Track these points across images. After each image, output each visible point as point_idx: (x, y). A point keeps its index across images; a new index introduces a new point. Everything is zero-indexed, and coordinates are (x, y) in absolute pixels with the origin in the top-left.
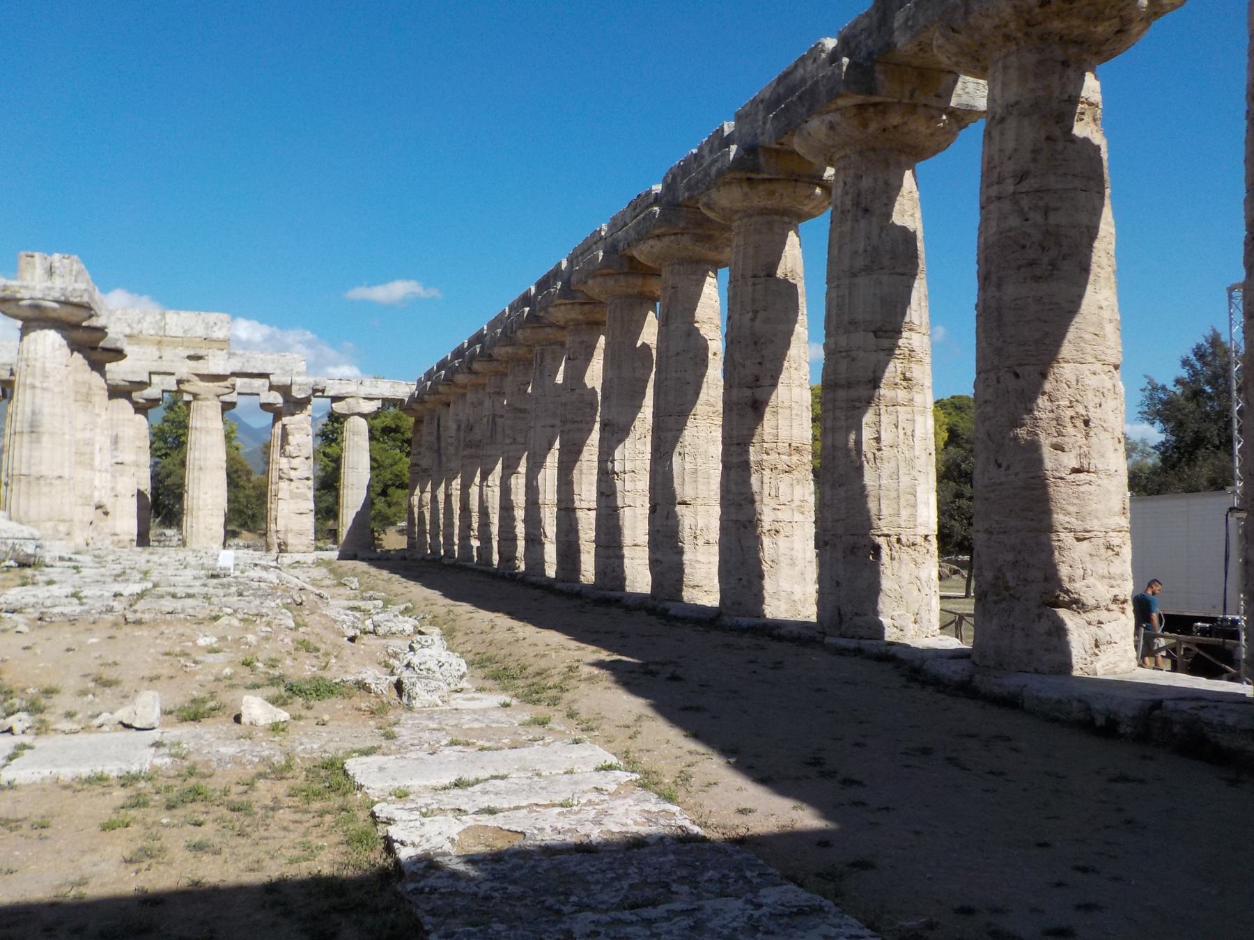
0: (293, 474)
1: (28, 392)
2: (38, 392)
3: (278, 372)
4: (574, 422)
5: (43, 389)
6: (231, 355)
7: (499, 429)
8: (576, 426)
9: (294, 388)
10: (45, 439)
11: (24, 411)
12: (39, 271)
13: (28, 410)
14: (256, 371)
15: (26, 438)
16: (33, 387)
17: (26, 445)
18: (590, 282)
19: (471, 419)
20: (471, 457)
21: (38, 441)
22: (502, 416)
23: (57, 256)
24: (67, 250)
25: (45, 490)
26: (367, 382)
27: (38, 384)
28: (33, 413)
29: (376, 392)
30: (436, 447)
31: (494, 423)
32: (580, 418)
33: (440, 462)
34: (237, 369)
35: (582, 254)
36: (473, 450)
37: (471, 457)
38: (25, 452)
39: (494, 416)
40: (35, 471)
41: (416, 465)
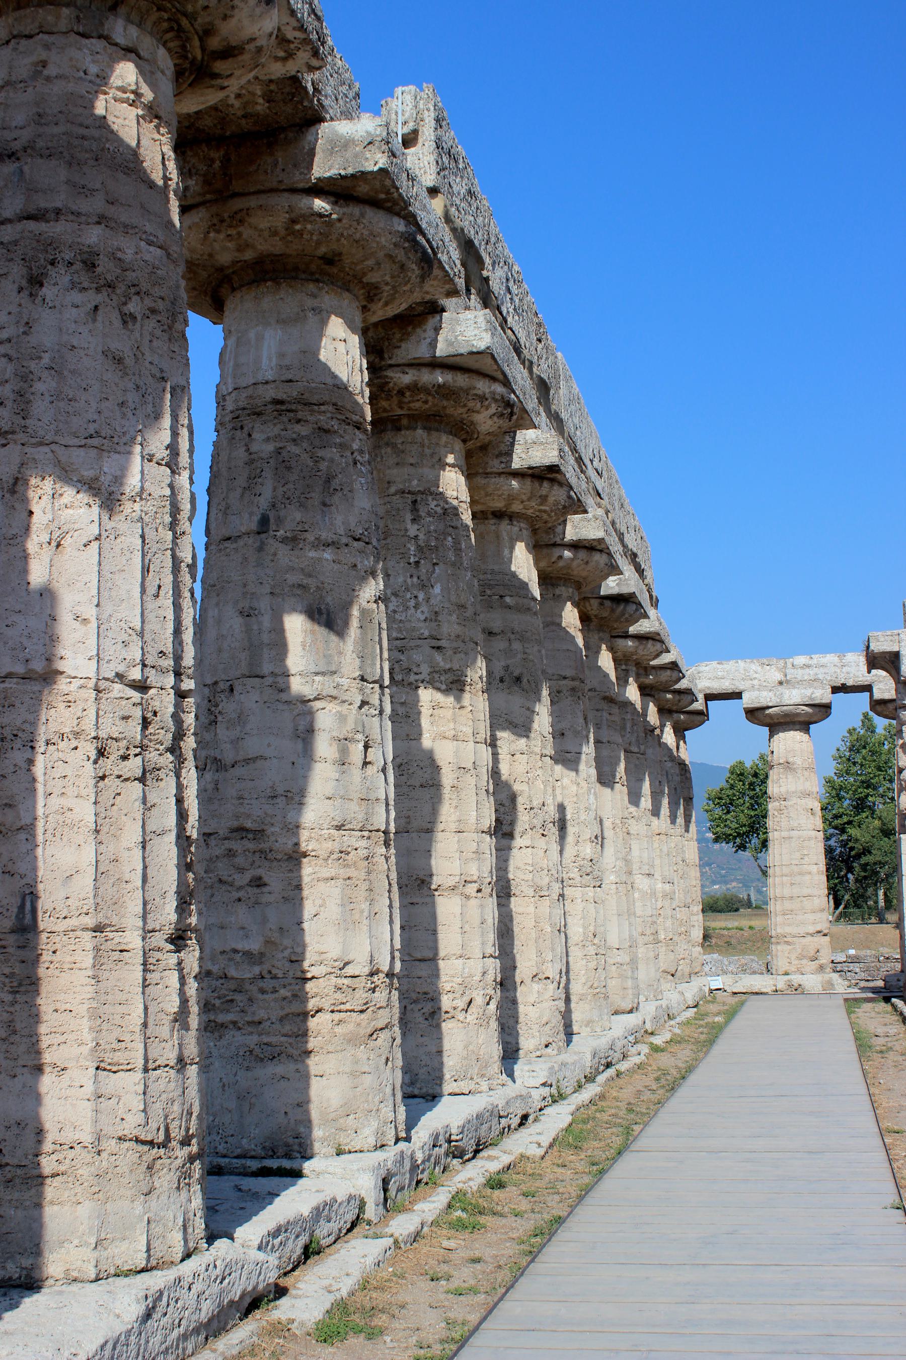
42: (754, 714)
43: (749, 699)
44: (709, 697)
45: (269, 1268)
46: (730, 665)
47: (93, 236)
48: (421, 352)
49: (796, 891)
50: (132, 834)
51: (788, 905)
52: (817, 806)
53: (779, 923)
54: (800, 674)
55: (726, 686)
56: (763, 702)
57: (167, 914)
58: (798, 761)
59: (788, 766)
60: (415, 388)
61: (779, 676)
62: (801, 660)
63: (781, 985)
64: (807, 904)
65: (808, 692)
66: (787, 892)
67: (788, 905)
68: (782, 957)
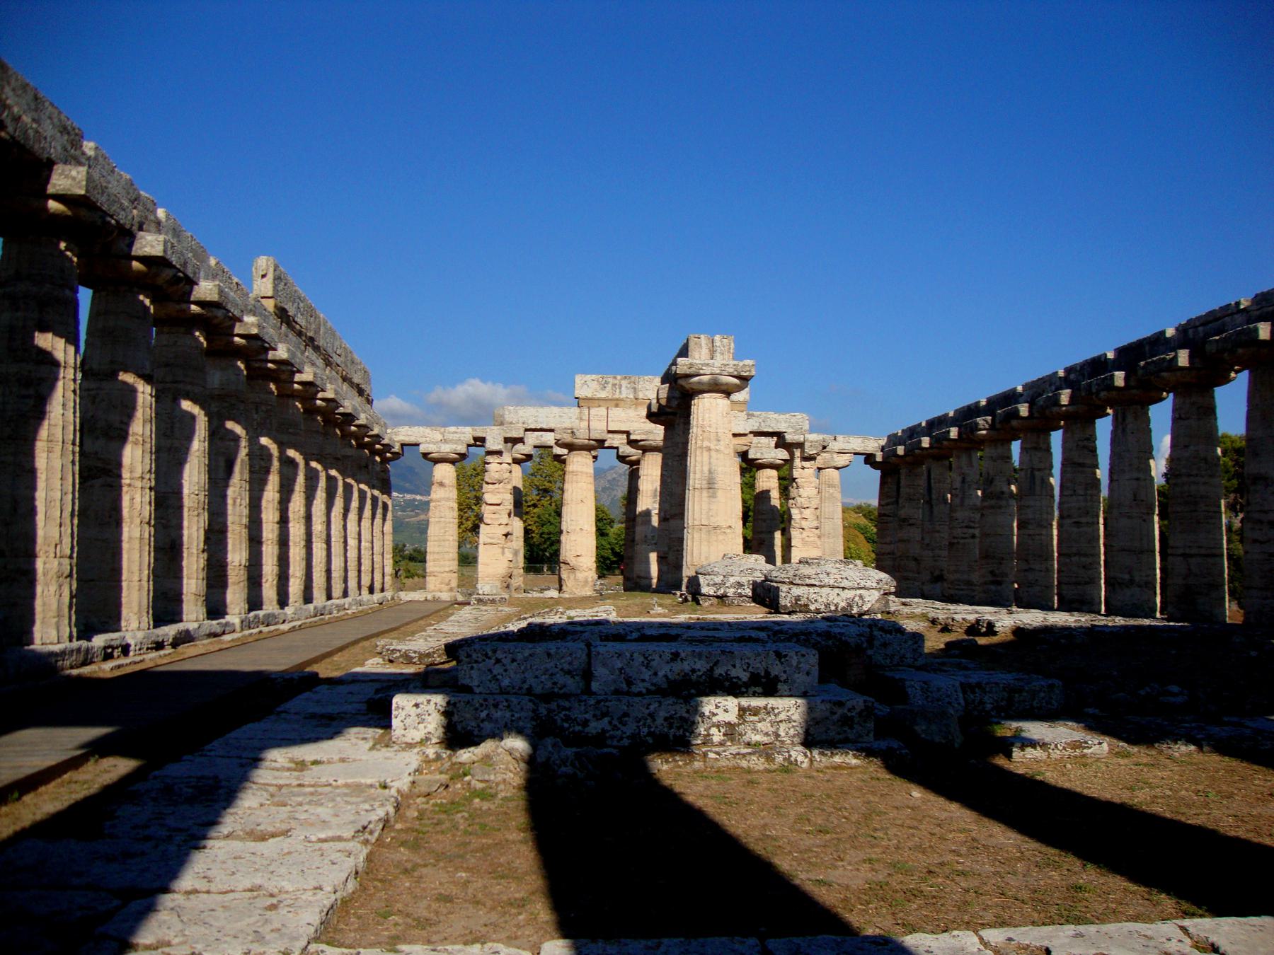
0: (804, 524)
1: (706, 454)
2: (713, 453)
3: (790, 430)
4: (1190, 475)
5: (717, 451)
6: (749, 416)
7: (1038, 482)
8: (1192, 479)
9: (807, 445)
10: (720, 493)
11: (702, 471)
12: (705, 351)
13: (706, 469)
14: (770, 430)
15: (705, 494)
16: (709, 449)
17: (705, 499)
18: (1240, 351)
19: (991, 472)
20: (992, 507)
21: (713, 496)
22: (1039, 470)
23: (717, 338)
24: (725, 333)
25: (721, 537)
26: (840, 438)
27: (712, 447)
28: (710, 472)
29: (848, 447)
30: (927, 498)
31: (1033, 477)
32: (1194, 472)
33: (932, 512)
34: (755, 428)
35: (1202, 325)
36: (993, 502)
37: (992, 507)
38: (705, 506)
39: (1033, 469)
40: (714, 521)
41: (885, 515)
42: (425, 455)
43: (422, 449)
44: (403, 445)
45: (219, 630)
46: (416, 429)
47: (189, 387)
48: (263, 357)
49: (441, 549)
50: (195, 528)
51: (436, 556)
52: (456, 506)
53: (431, 566)
54: (451, 436)
55: (412, 440)
56: (430, 450)
57: (202, 545)
58: (446, 481)
59: (441, 484)
60: (259, 368)
61: (440, 437)
62: (453, 429)
63: (429, 597)
64: (446, 556)
65: (454, 446)
66: (437, 549)
67: (436, 556)
68: (431, 582)
